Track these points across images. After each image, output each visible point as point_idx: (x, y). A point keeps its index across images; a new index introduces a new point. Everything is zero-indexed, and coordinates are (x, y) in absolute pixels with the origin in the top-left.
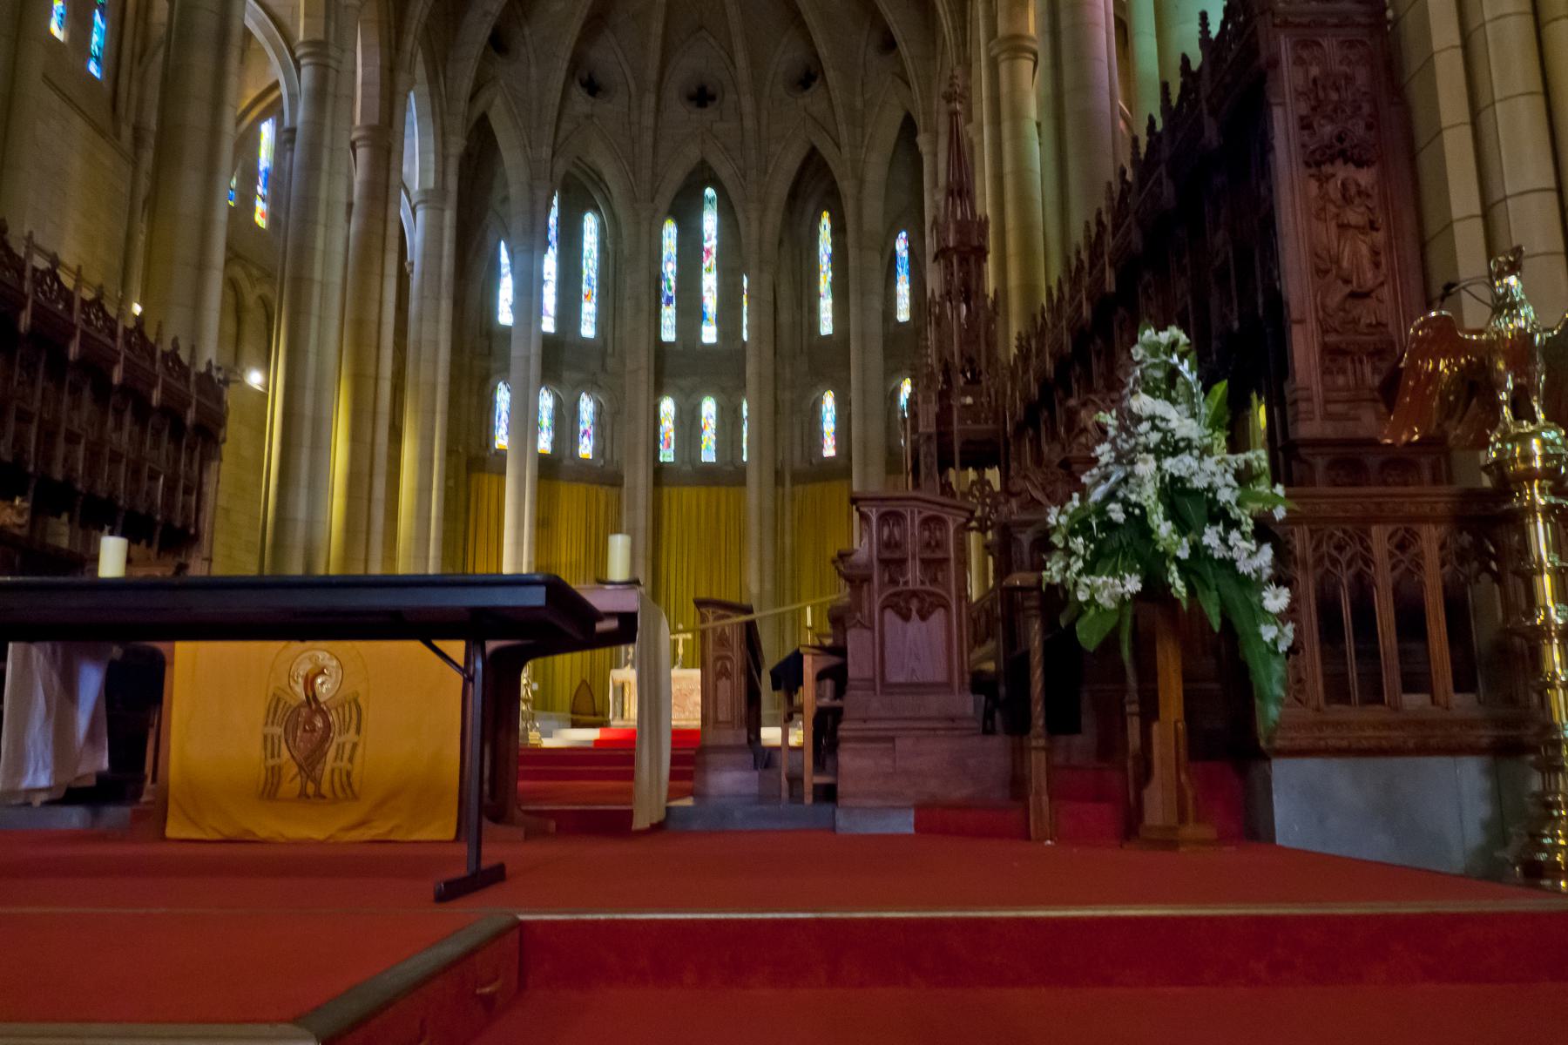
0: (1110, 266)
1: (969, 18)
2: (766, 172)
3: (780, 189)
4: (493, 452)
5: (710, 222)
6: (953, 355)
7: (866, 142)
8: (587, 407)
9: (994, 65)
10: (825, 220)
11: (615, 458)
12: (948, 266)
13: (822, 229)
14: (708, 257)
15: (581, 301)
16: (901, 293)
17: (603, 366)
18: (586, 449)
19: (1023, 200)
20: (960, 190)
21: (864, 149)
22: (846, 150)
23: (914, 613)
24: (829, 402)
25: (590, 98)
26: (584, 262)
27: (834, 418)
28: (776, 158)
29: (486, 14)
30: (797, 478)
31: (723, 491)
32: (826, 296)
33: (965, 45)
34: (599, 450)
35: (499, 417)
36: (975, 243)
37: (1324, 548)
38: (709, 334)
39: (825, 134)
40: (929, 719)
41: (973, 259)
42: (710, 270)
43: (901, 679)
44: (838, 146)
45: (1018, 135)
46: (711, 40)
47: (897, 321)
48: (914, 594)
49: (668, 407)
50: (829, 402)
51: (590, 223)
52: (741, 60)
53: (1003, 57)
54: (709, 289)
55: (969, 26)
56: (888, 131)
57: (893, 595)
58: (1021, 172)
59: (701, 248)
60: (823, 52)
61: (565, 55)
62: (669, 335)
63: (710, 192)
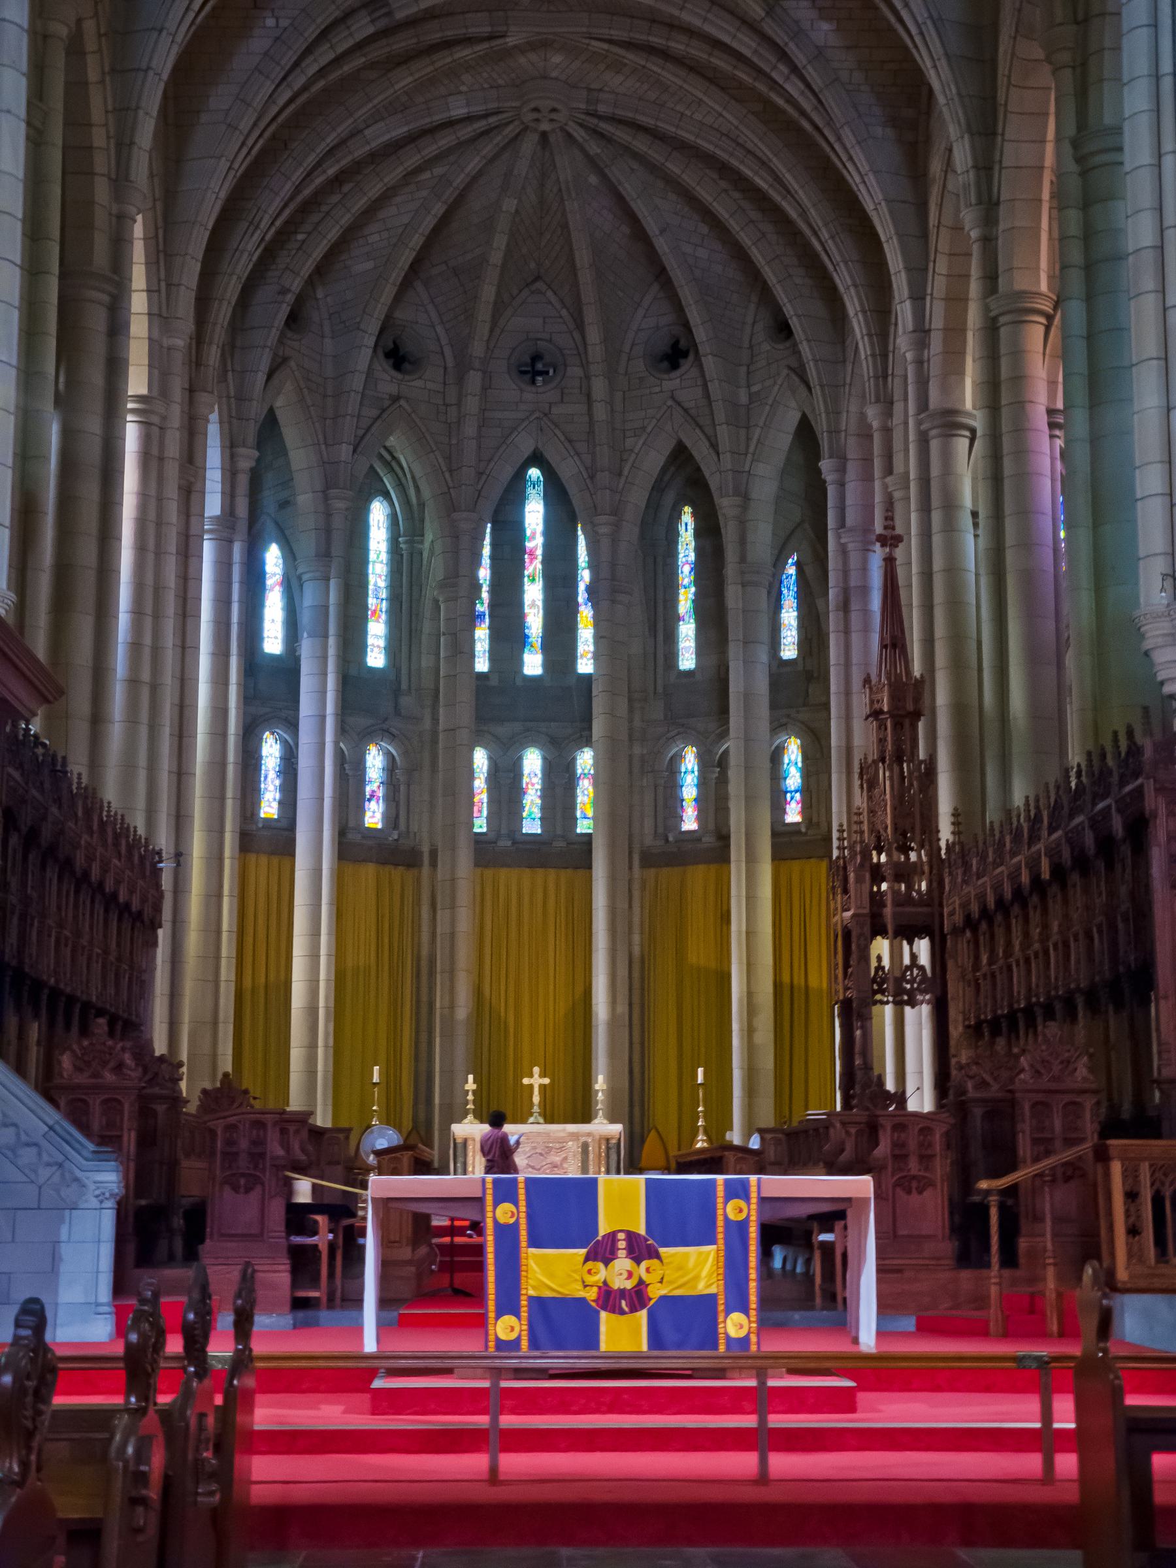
0: (1046, 855)
1: (891, 348)
2: (620, 474)
3: (638, 497)
4: (260, 825)
5: (534, 514)
6: (886, 827)
7: (751, 450)
8: (375, 761)
9: (924, 440)
10: (687, 517)
11: (414, 827)
12: (882, 726)
13: (682, 529)
14: (531, 562)
15: (365, 620)
16: (786, 622)
17: (397, 712)
18: (374, 816)
19: (955, 604)
20: (895, 643)
21: (749, 457)
22: (727, 460)
23: (914, 1190)
24: (690, 761)
25: (399, 376)
26: (371, 566)
27: (696, 781)
28: (633, 456)
29: (284, 291)
30: (649, 860)
31: (552, 872)
32: (686, 618)
33: (885, 377)
34: (391, 818)
35: (266, 777)
36: (910, 707)
37: (1157, 1175)
38: (533, 664)
39: (698, 431)
40: (924, 1258)
41: (907, 722)
42: (534, 579)
43: (905, 1232)
44: (714, 446)
45: (950, 527)
46: (550, 294)
47: (781, 658)
48: (914, 1177)
49: (480, 759)
50: (690, 761)
51: (378, 514)
52: (594, 335)
53: (933, 433)
54: (533, 605)
55: (891, 355)
56: (782, 439)
57: (899, 1178)
58: (953, 570)
59: (523, 550)
60: (701, 334)
61: (373, 327)
62: (482, 665)
63: (534, 473)
